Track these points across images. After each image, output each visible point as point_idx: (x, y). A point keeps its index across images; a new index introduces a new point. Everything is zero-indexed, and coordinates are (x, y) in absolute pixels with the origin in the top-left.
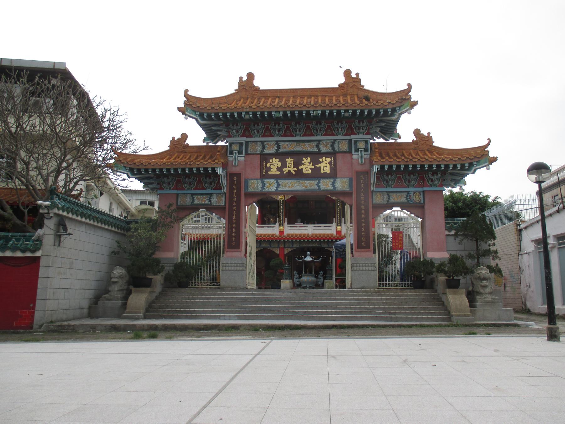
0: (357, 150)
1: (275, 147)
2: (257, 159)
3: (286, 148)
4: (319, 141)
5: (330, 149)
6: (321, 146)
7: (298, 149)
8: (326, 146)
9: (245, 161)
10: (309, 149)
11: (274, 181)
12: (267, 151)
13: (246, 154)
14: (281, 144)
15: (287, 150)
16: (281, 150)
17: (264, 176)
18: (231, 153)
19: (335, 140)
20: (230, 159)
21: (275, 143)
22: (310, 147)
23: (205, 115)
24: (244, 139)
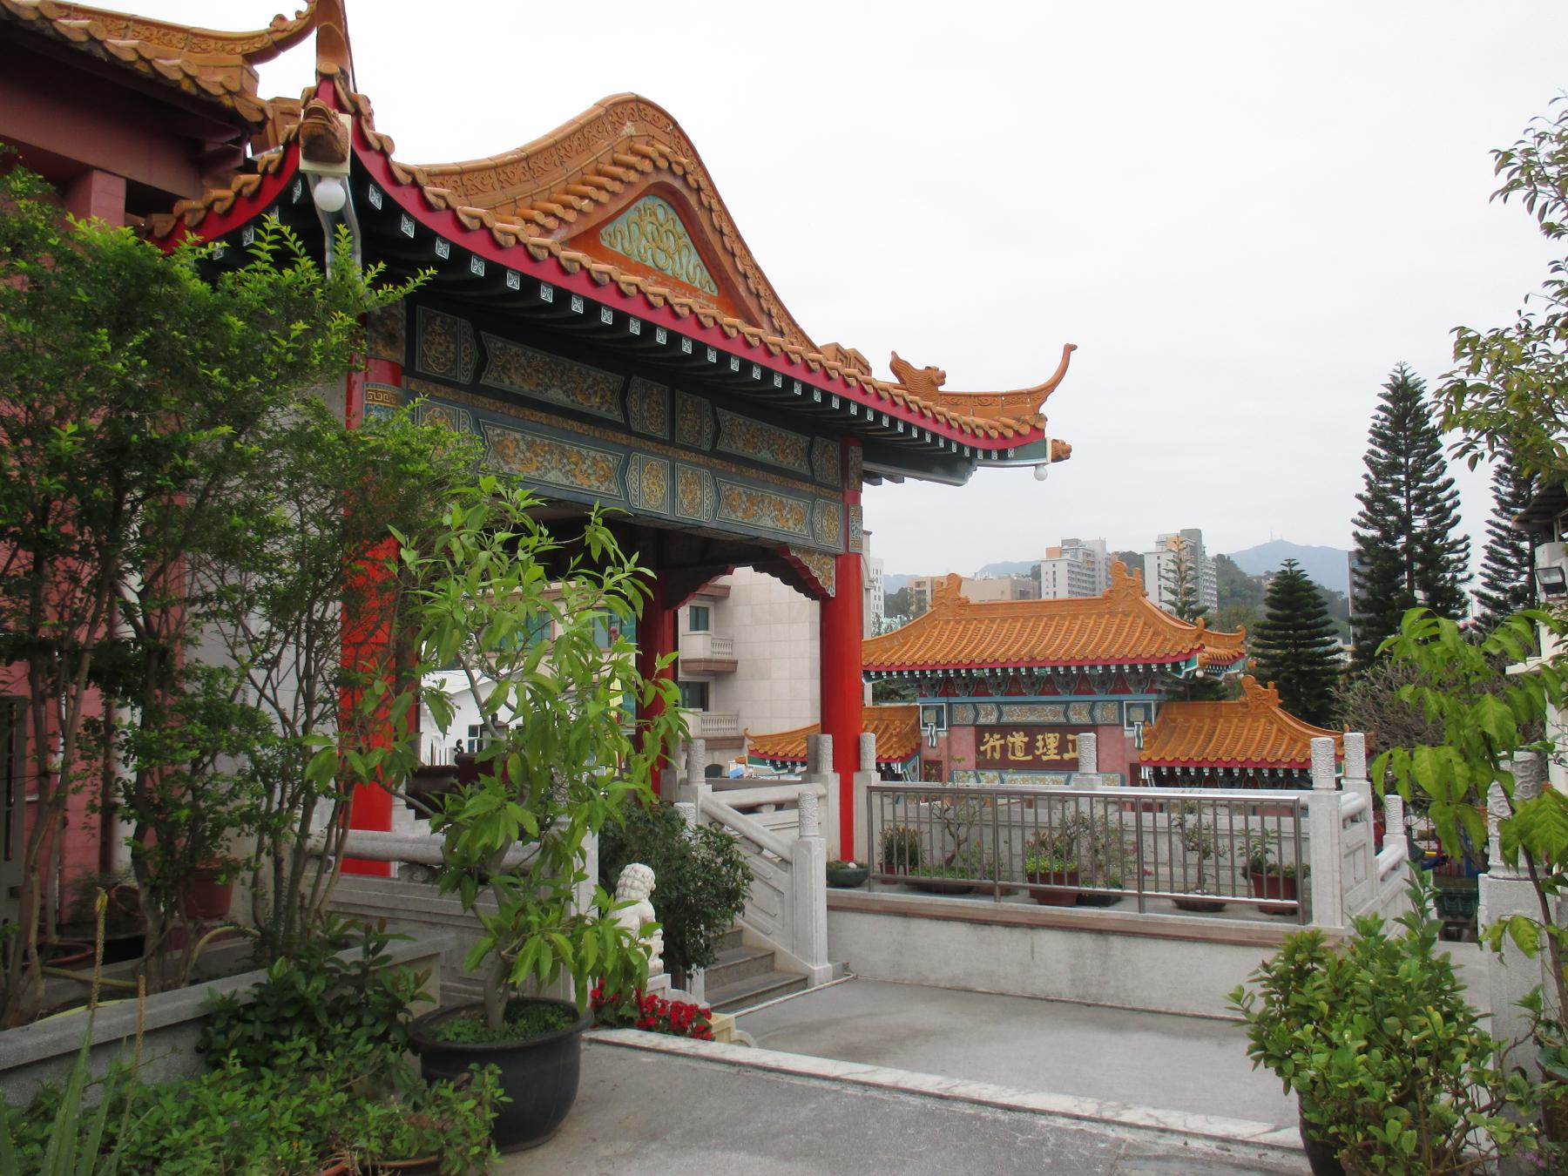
0: (1131, 724)
1: (995, 714)
2: (968, 736)
3: (1015, 715)
4: (1068, 703)
5: (1086, 720)
6: (1071, 714)
7: (1032, 718)
8: (1080, 714)
9: (948, 738)
10: (1052, 719)
11: (995, 773)
12: (982, 721)
13: (949, 726)
14: (1005, 709)
15: (1015, 719)
16: (1005, 719)
17: (983, 764)
18: (925, 725)
19: (1094, 703)
20: (924, 734)
21: (994, 706)
22: (1049, 715)
23: (873, 674)
24: (942, 701)
